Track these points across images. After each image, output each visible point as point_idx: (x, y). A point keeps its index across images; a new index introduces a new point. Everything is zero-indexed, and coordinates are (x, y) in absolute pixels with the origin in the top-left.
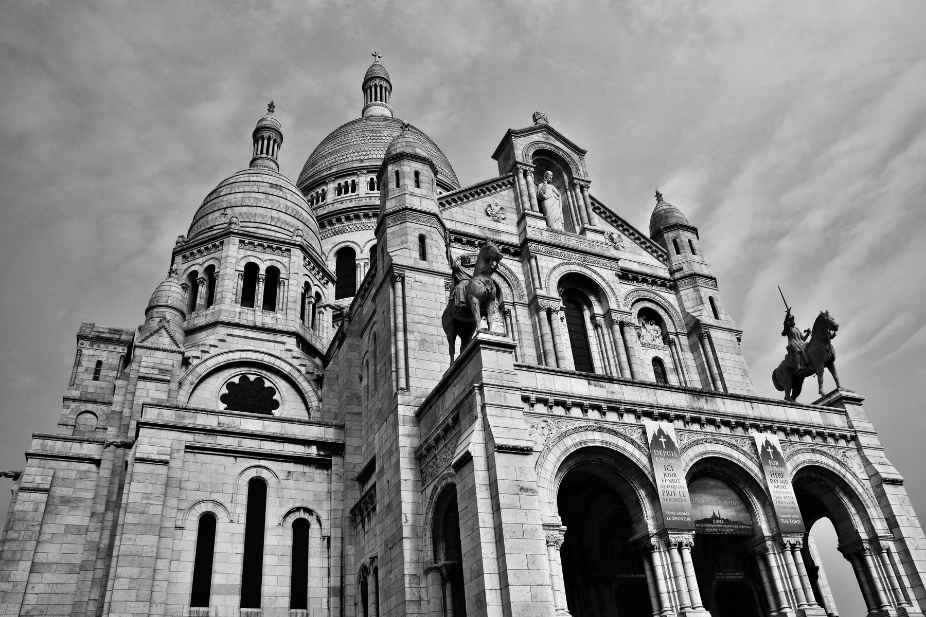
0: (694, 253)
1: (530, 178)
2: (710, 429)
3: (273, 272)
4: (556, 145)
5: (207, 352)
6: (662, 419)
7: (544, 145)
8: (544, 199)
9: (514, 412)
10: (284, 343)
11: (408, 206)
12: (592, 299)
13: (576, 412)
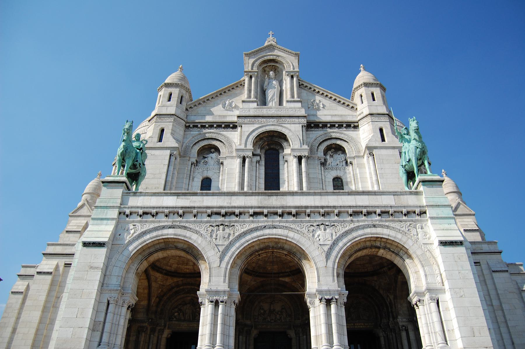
4: (278, 54)
6: (230, 215)
7: (268, 57)
8: (266, 89)
9: (109, 222)
12: (285, 144)
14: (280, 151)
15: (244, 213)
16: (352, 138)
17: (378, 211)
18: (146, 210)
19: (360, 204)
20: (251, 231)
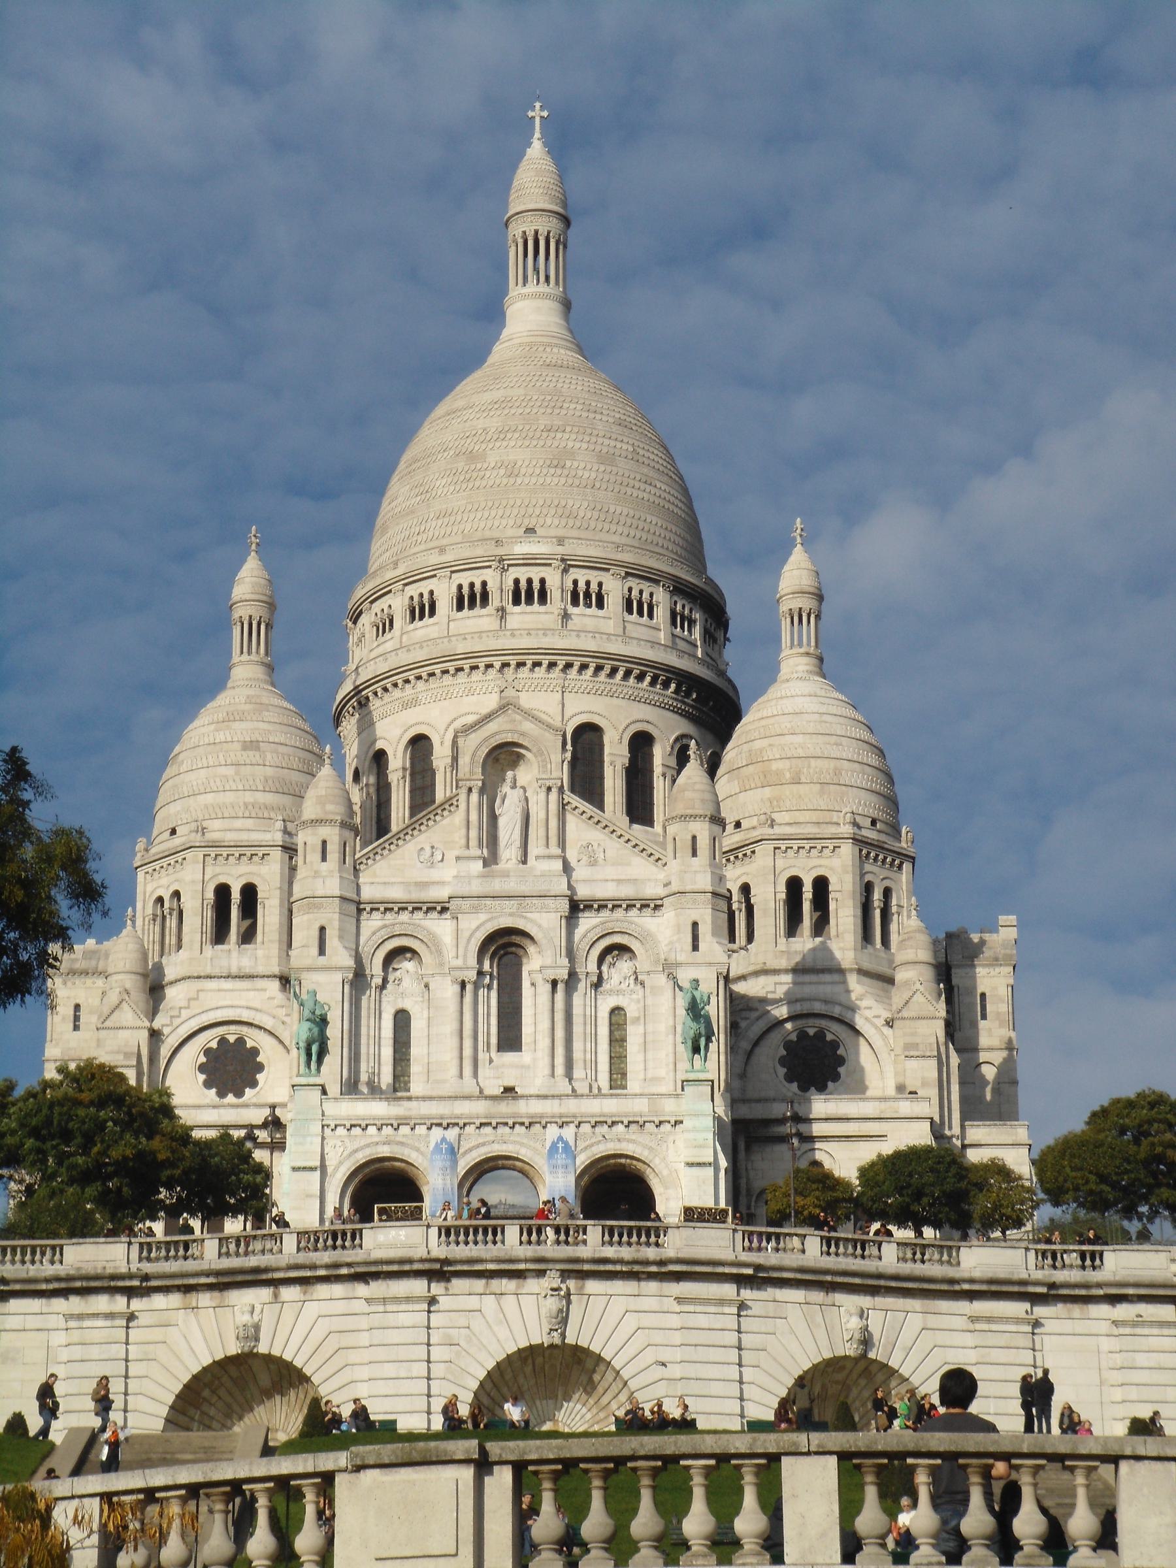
0: (694, 854)
1: (474, 797)
2: (503, 1130)
3: (250, 892)
5: (179, 1017)
7: (504, 735)
10: (265, 990)
11: (309, 894)
12: (531, 949)
13: (372, 1130)
14: (525, 960)
15: (470, 1124)
16: (649, 934)
17: (626, 1122)
18: (354, 1122)
19: (606, 1110)
20: (478, 1146)
